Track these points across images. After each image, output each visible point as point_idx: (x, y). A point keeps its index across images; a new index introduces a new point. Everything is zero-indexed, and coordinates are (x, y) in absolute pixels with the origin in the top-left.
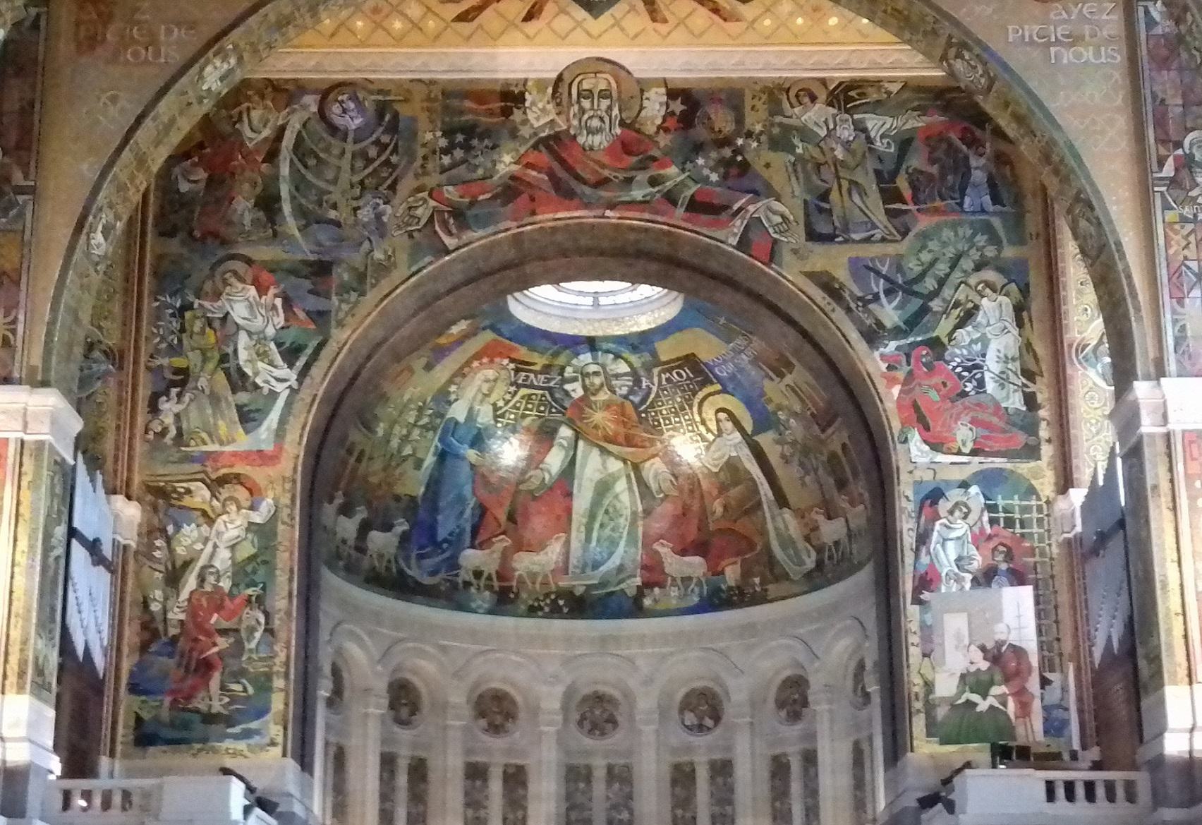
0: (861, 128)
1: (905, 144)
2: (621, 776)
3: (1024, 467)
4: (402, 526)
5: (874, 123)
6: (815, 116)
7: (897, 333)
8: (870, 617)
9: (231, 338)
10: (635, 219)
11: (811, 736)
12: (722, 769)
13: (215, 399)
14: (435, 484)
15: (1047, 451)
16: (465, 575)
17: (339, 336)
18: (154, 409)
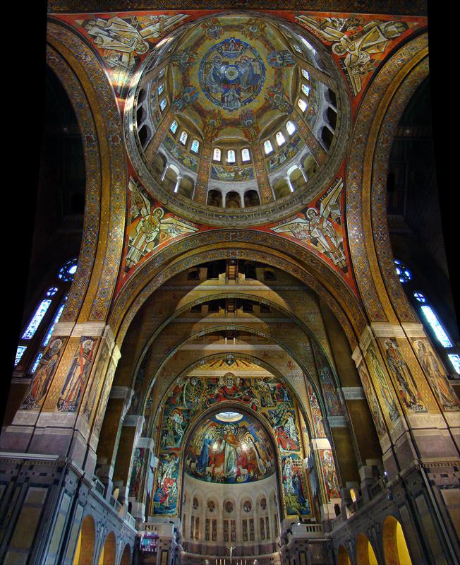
0: (268, 386)
1: (275, 388)
2: (233, 523)
3: (298, 453)
4: (197, 462)
5: (270, 384)
6: (261, 383)
7: (276, 425)
8: (276, 485)
9: (174, 425)
10: (236, 402)
11: (267, 514)
12: (252, 521)
13: (171, 437)
14: (202, 452)
15: (301, 449)
16: (207, 473)
17: (191, 424)
18: (162, 439)
